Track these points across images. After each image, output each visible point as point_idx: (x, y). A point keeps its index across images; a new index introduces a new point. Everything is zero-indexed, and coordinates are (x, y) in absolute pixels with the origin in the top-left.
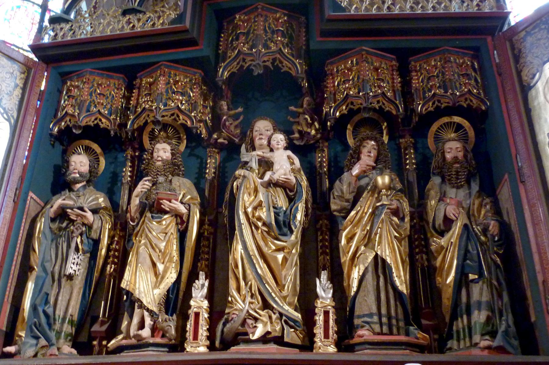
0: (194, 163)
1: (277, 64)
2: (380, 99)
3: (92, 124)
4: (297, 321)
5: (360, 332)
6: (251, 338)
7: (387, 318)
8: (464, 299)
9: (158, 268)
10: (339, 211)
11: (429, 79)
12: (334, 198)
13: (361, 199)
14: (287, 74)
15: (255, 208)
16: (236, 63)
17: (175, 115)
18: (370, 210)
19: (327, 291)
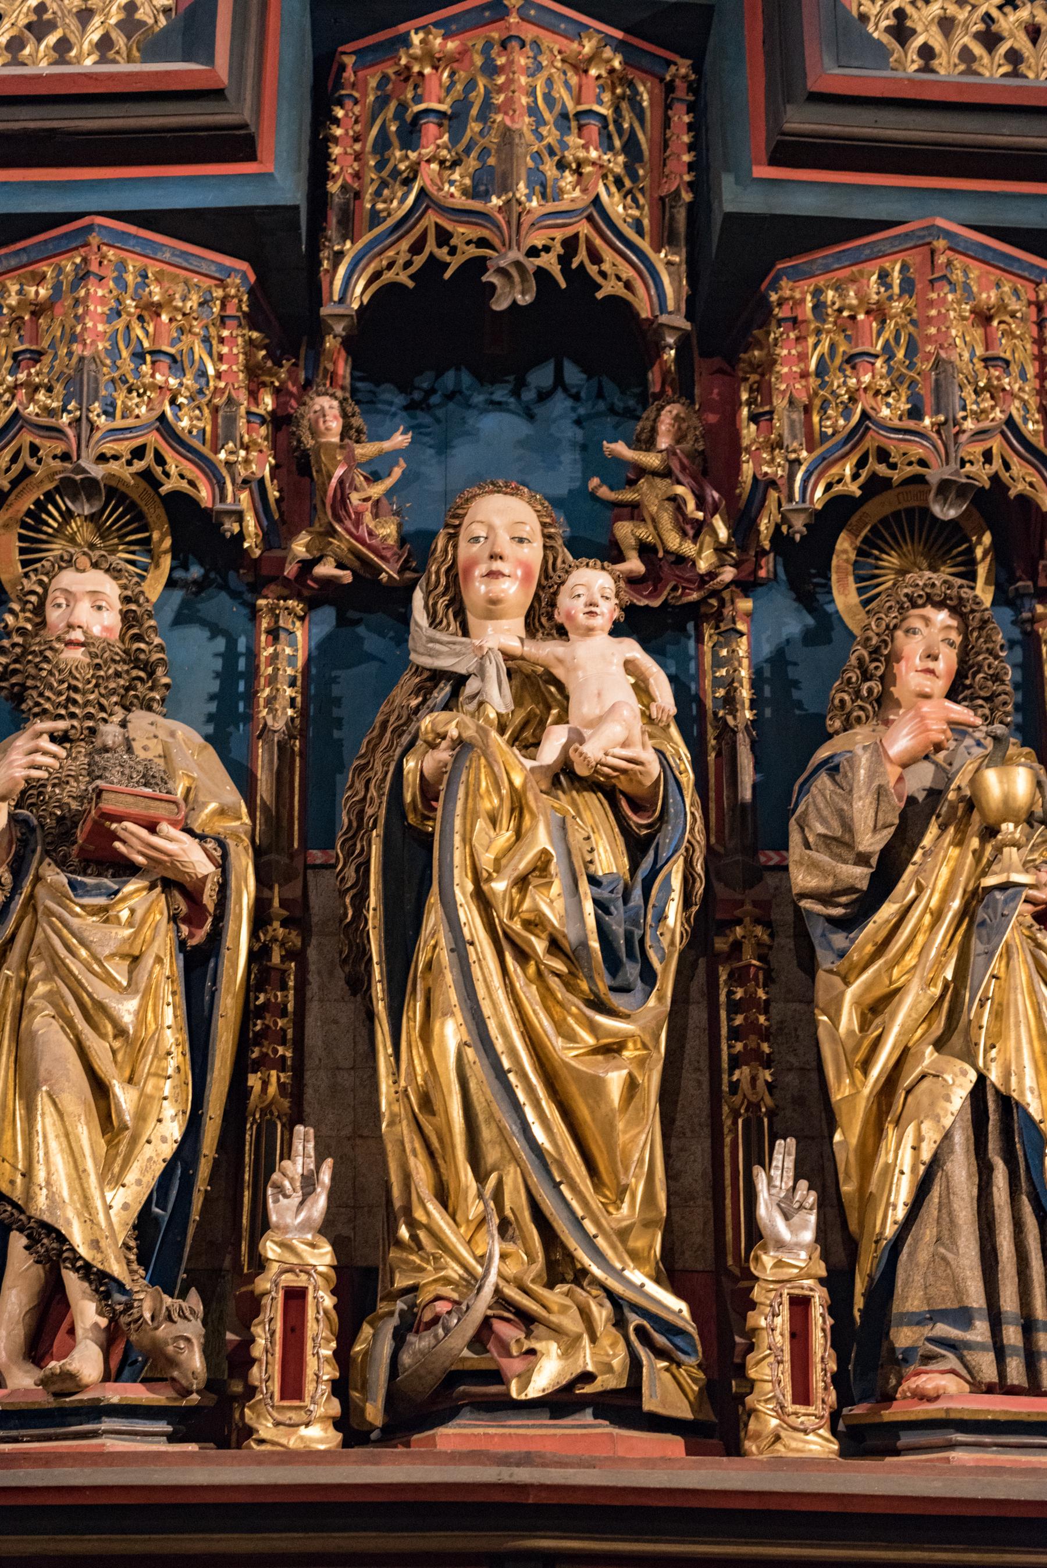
1: (582, 265)
2: (996, 444)
4: (680, 1332)
6: (514, 1395)
7: (1020, 1329)
9: (118, 1105)
10: (826, 898)
12: (807, 846)
13: (917, 857)
14: (620, 306)
15: (522, 882)
16: (405, 245)
17: (150, 455)
18: (956, 904)
19: (796, 1219)
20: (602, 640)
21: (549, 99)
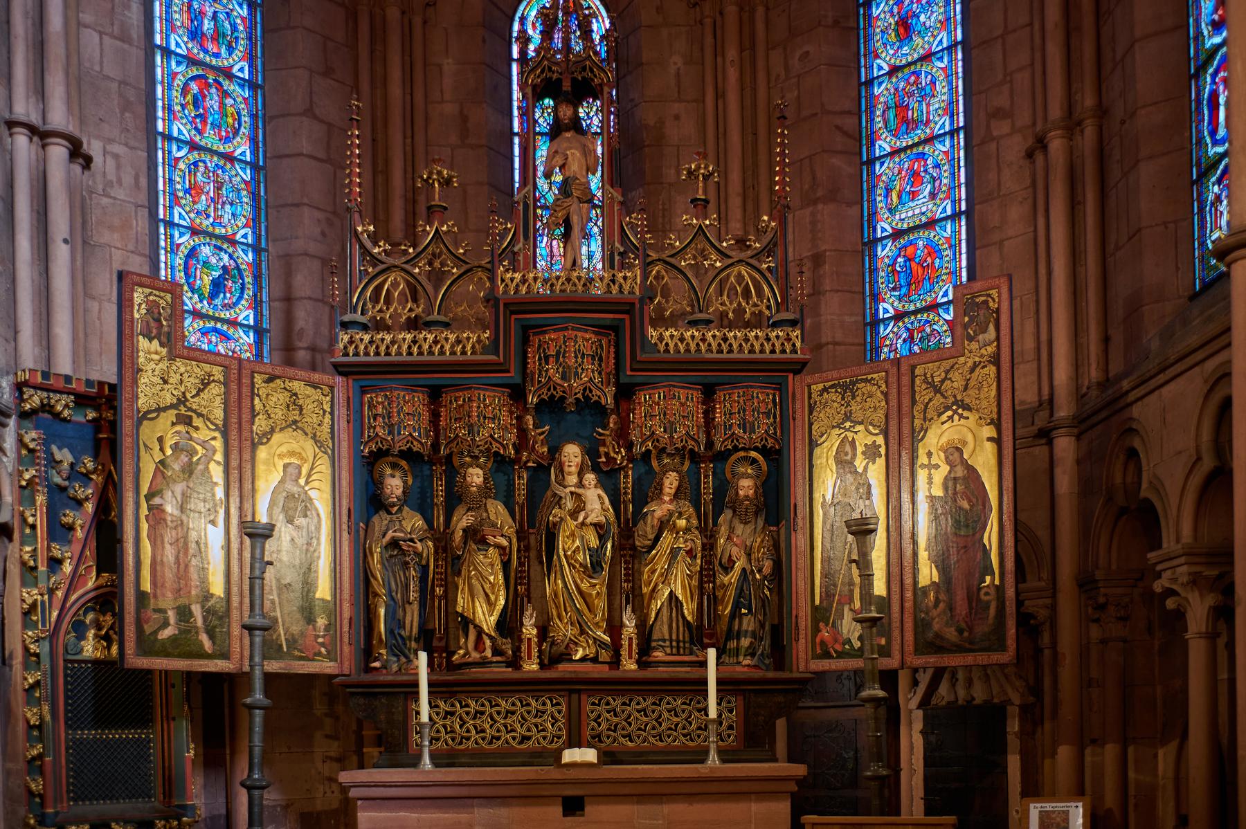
0: (502, 478)
5: (656, 654)
8: (736, 628)
11: (731, 414)
15: (574, 552)
20: (593, 490)
21: (579, 350)
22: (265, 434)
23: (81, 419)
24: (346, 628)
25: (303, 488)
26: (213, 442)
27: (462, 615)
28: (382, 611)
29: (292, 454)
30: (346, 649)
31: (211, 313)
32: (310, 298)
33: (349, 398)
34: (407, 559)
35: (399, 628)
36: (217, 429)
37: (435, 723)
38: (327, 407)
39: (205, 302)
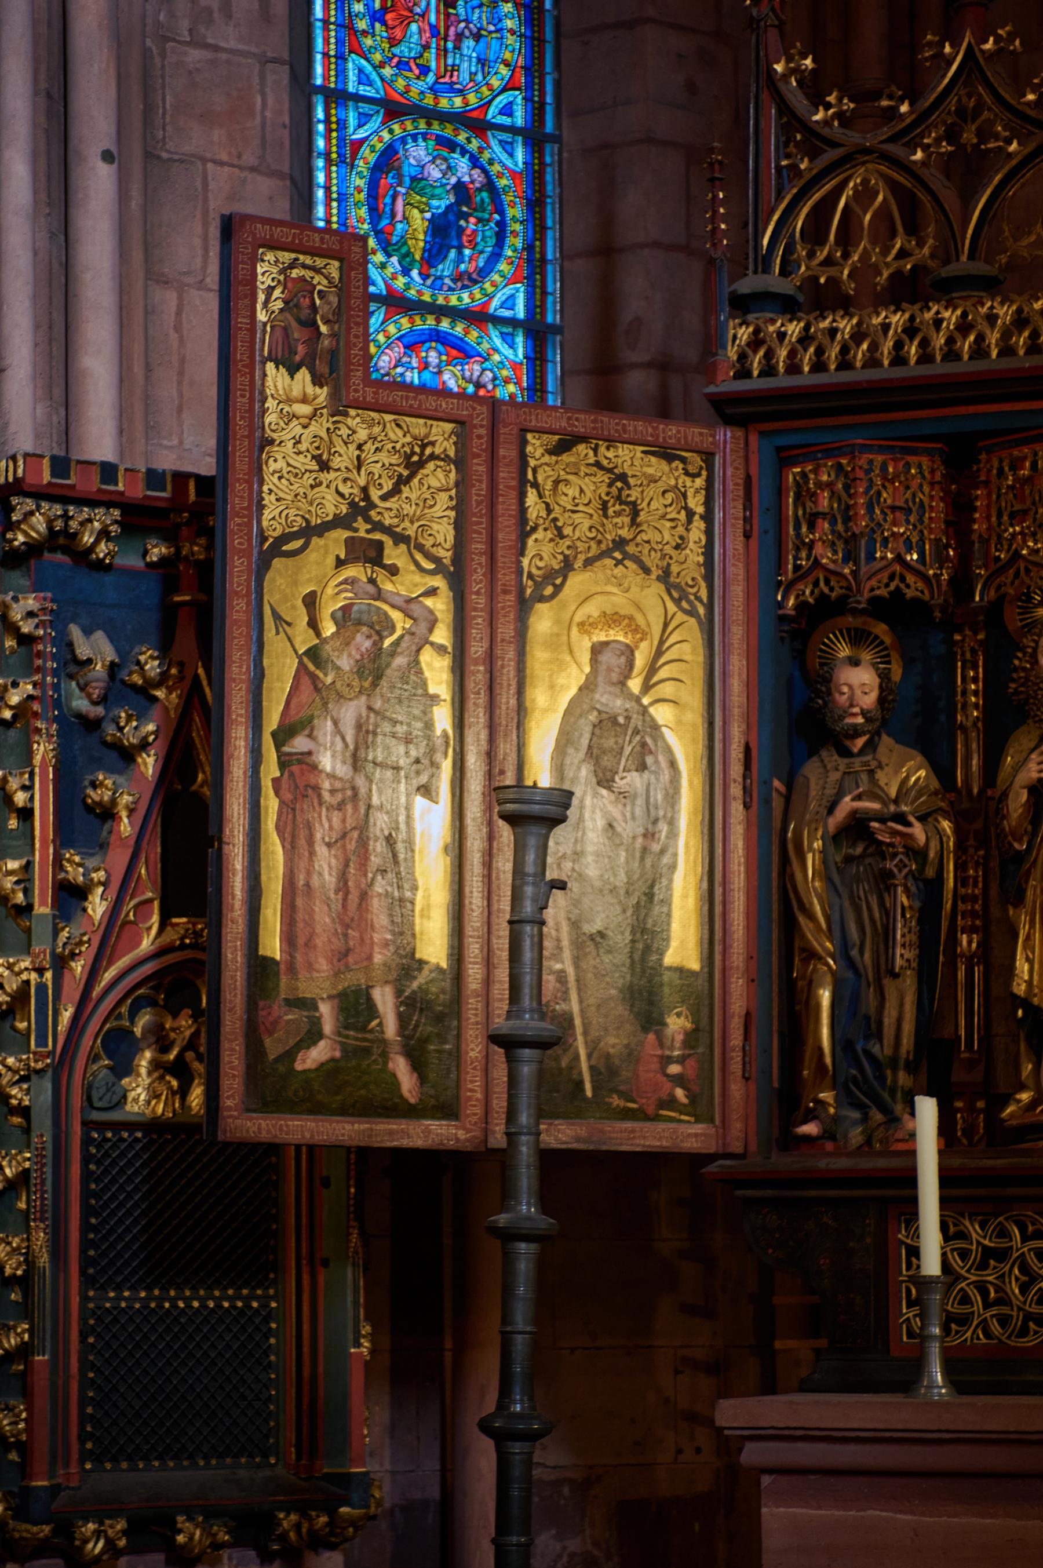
3: (883, 592)
22: (549, 576)
23: (134, 561)
24: (736, 1039)
25: (638, 700)
26: (429, 602)
27: (1024, 1003)
28: (825, 996)
29: (612, 619)
30: (737, 1089)
31: (426, 298)
32: (656, 245)
33: (748, 479)
34: (889, 865)
35: (867, 1037)
36: (440, 568)
37: (959, 1278)
38: (697, 504)
39: (415, 274)
